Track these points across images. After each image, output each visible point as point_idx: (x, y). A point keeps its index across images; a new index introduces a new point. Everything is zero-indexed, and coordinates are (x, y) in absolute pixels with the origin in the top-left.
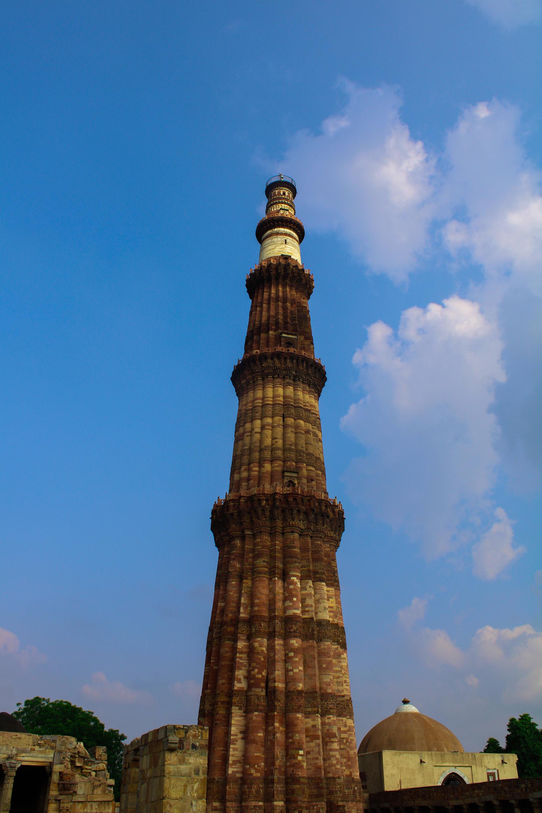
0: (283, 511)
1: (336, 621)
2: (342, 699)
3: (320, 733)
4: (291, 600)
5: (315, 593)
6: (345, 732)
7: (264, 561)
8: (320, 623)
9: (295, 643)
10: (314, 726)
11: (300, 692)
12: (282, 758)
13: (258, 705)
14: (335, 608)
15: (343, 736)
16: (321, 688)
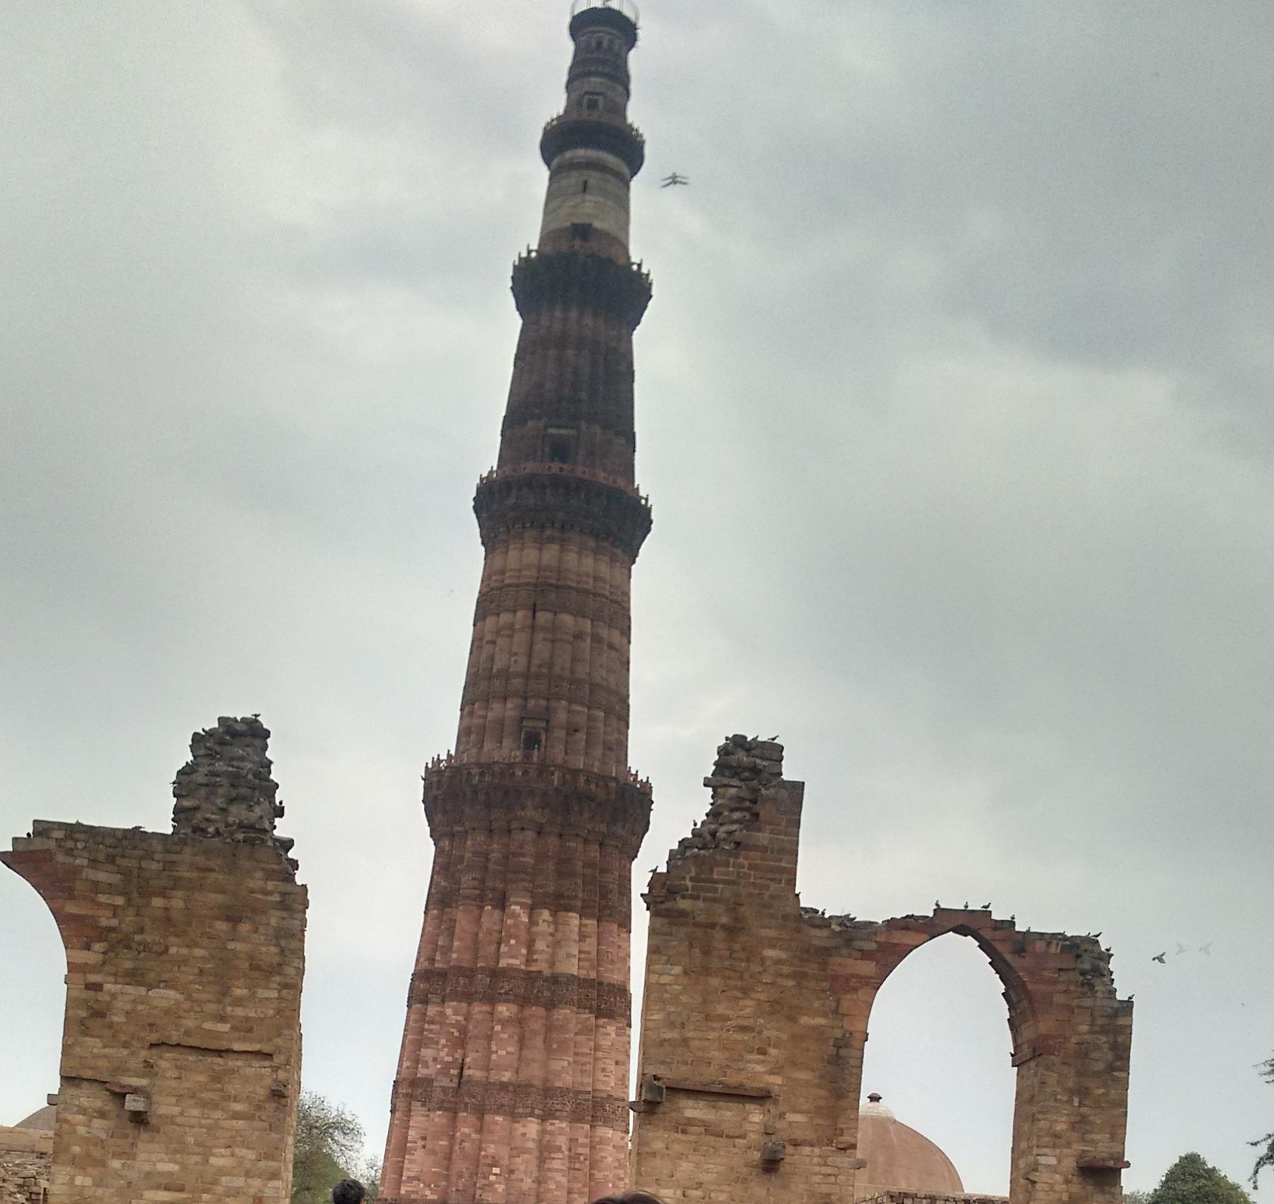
0: (506, 793)
1: (593, 975)
2: (587, 1097)
3: (531, 1145)
4: (508, 944)
5: (556, 930)
6: (583, 1145)
7: (474, 879)
8: (555, 980)
9: (503, 1010)
10: (524, 1135)
11: (503, 1086)
12: (471, 1177)
13: (443, 1101)
14: (594, 954)
15: (580, 1150)
16: (546, 1080)
